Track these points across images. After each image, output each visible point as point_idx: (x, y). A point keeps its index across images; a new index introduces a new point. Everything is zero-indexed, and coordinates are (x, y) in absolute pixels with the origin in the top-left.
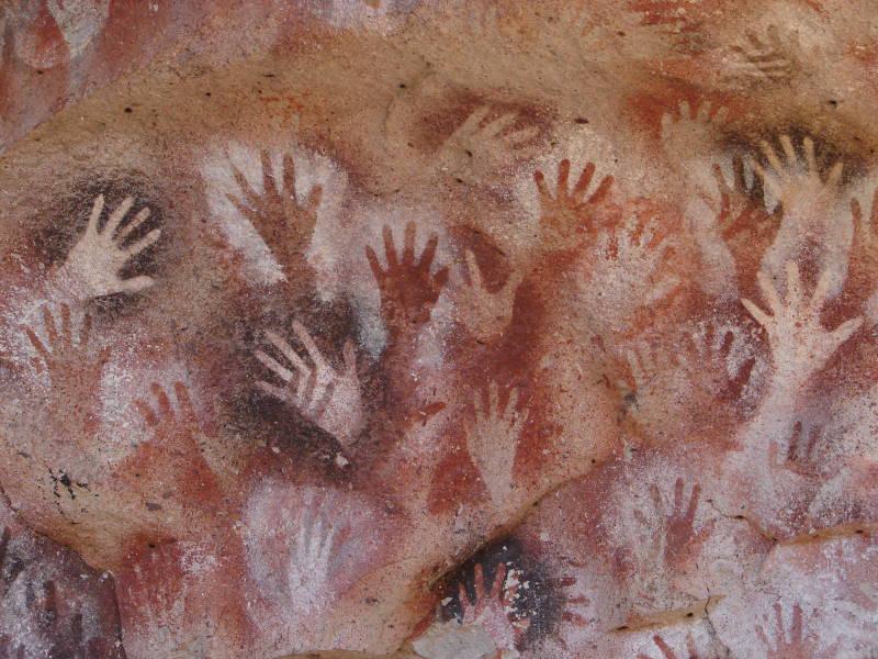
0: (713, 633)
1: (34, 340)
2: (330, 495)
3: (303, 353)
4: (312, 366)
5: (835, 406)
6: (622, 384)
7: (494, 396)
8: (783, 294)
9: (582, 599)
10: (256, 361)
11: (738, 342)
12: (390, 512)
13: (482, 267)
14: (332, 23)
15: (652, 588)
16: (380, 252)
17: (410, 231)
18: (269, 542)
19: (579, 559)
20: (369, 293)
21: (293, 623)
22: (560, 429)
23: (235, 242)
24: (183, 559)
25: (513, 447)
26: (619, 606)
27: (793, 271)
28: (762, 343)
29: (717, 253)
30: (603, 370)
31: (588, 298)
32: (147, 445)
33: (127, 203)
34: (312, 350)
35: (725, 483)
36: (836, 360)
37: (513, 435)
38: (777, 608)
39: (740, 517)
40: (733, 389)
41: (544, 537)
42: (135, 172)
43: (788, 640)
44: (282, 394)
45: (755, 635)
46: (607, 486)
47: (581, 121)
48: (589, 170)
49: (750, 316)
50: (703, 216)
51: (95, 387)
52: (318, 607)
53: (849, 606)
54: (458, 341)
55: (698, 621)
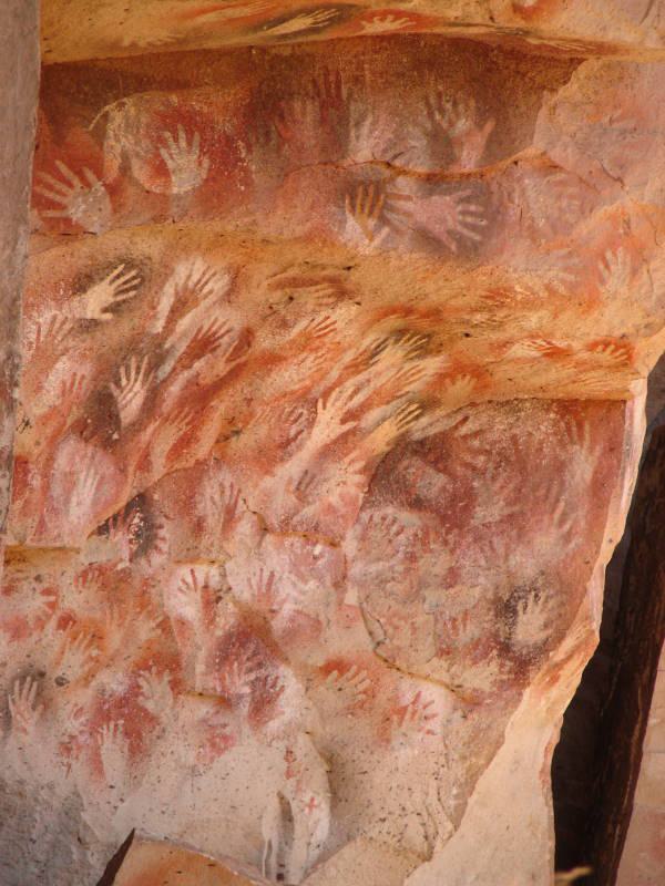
0: (224, 576)
1: (39, 331)
2: (100, 453)
3: (138, 373)
4: (136, 380)
5: (324, 466)
6: (240, 425)
7: (182, 415)
8: (336, 400)
9: (163, 539)
10: (118, 372)
11: (303, 419)
12: (120, 470)
13: (234, 349)
14: (340, 238)
15: (212, 545)
16: (205, 328)
17: (224, 323)
18: (65, 475)
19: (172, 516)
20: (182, 348)
21: (66, 528)
22: (198, 441)
23: (159, 308)
24: (30, 475)
25: (171, 444)
26: (188, 550)
27: (352, 389)
28: (311, 423)
29: (335, 374)
30: (237, 415)
31: (269, 380)
32: (55, 407)
33: (133, 273)
34: (142, 371)
35: (257, 493)
36: (335, 442)
37: (176, 437)
38: (262, 570)
39: (254, 513)
40: (289, 442)
41: (156, 497)
42: (150, 258)
43: (264, 590)
44: (116, 393)
45: (246, 582)
46: (200, 478)
47: (358, 304)
48: (335, 322)
49: (316, 407)
50: (348, 357)
51: (51, 367)
52: (82, 521)
53: (293, 578)
54: (193, 382)
55: (216, 566)
